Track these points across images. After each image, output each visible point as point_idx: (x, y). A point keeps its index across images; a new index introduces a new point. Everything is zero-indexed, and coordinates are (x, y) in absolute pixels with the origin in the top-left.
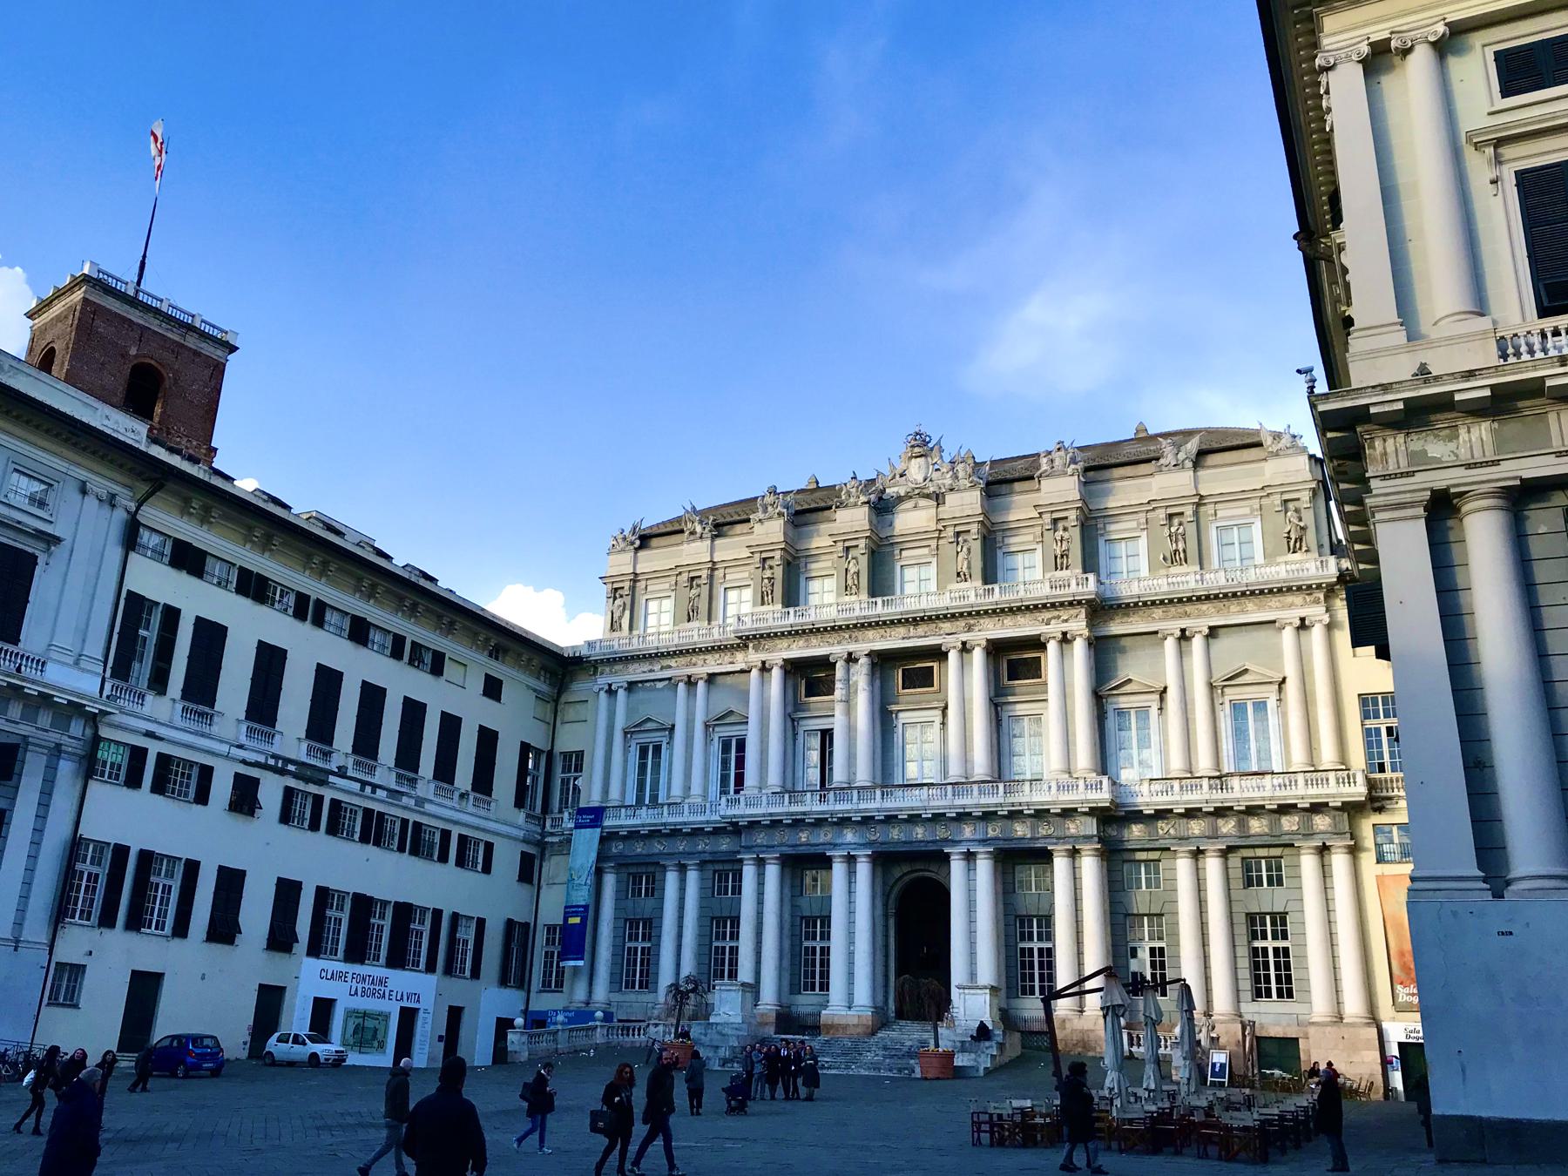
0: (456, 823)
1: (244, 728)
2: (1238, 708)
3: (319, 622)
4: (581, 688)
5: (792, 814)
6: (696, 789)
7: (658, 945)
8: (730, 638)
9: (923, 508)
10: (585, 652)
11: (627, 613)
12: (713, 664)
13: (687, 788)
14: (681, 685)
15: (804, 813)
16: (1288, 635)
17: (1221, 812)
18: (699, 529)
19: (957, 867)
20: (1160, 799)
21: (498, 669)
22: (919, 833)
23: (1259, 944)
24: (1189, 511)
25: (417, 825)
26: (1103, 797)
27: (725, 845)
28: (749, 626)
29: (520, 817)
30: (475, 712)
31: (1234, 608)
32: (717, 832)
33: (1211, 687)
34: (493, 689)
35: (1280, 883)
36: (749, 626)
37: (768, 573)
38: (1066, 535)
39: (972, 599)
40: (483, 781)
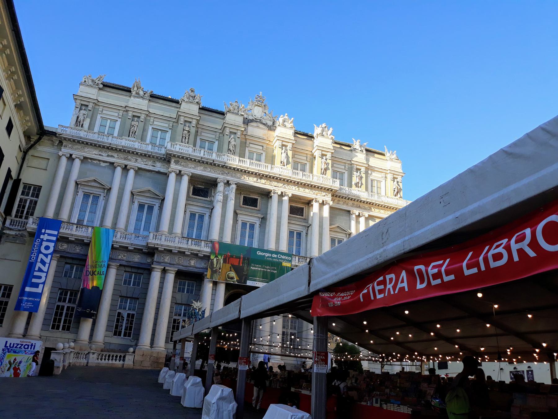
5: (192, 250)
6: (122, 224)
9: (262, 129)
10: (59, 131)
12: (141, 164)
14: (119, 170)
15: (199, 251)
18: (141, 93)
24: (363, 169)
27: (137, 258)
32: (138, 251)
37: (187, 129)
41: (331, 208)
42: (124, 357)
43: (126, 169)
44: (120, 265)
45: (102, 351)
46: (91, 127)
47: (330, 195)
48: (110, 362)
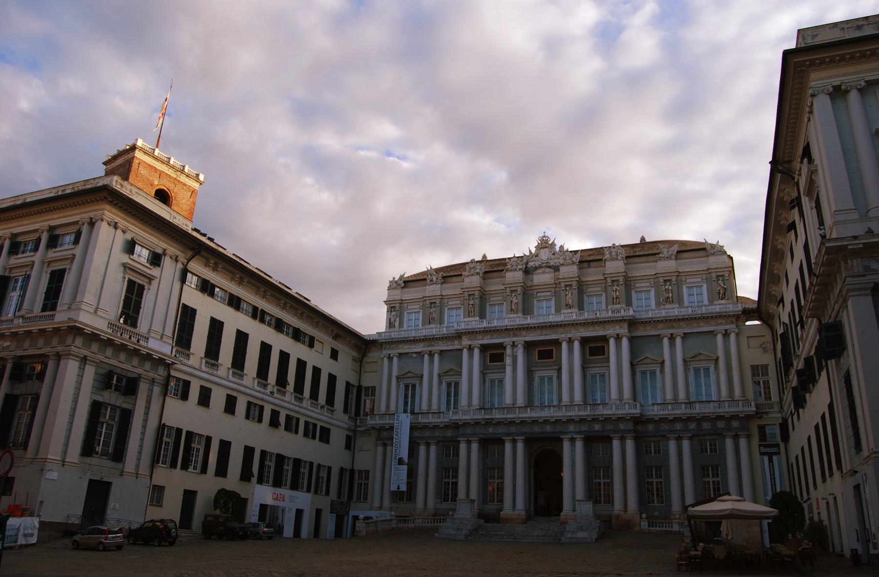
0: (319, 420)
1: (231, 372)
2: (697, 371)
3: (262, 321)
4: (373, 355)
6: (435, 407)
7: (416, 481)
8: (452, 331)
11: (398, 319)
13: (430, 405)
14: (426, 356)
16: (719, 338)
17: (690, 419)
18: (434, 279)
19: (566, 445)
20: (662, 413)
21: (339, 346)
22: (548, 428)
23: (706, 480)
26: (637, 411)
27: (449, 433)
28: (463, 327)
29: (346, 418)
30: (328, 367)
31: (695, 325)
32: (446, 427)
33: (685, 361)
34: (334, 355)
35: (716, 451)
36: (463, 326)
37: (472, 302)
39: (574, 317)
40: (330, 400)
41: (631, 340)
43: (431, 355)
44: (439, 442)
46: (401, 325)
47: (626, 325)
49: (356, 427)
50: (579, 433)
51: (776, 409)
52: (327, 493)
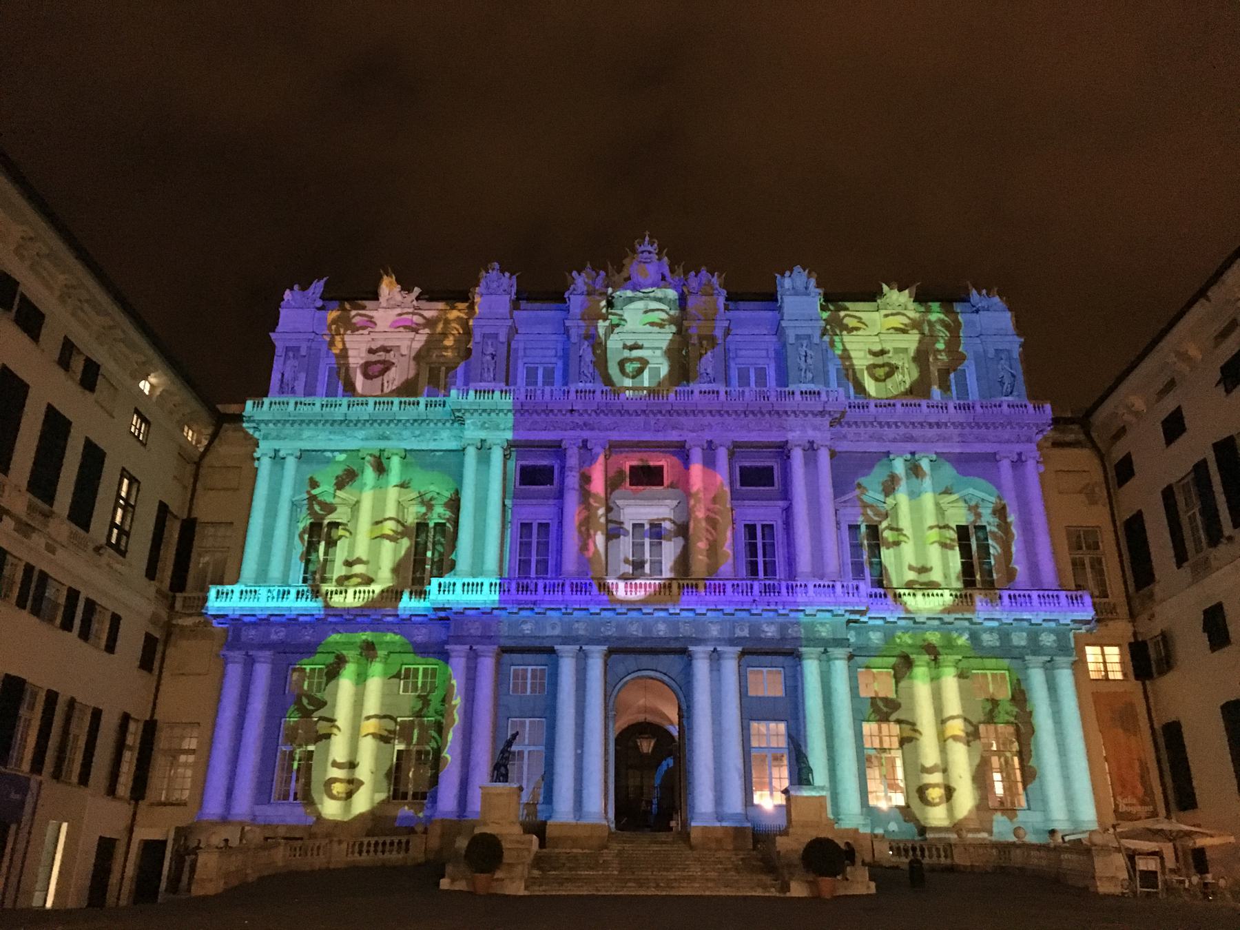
11: (303, 376)
25: (44, 577)
29: (151, 588)
37: (490, 350)
38: (809, 352)
42: (408, 842)
45: (367, 835)
48: (380, 854)
49: (170, 618)
50: (732, 642)
51: (1123, 610)
52: (84, 779)
